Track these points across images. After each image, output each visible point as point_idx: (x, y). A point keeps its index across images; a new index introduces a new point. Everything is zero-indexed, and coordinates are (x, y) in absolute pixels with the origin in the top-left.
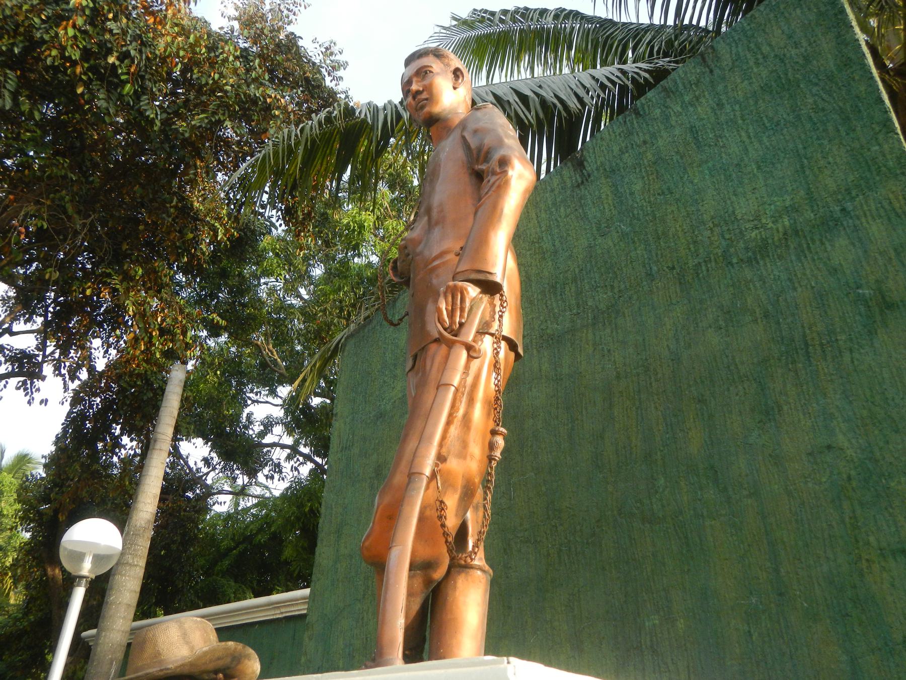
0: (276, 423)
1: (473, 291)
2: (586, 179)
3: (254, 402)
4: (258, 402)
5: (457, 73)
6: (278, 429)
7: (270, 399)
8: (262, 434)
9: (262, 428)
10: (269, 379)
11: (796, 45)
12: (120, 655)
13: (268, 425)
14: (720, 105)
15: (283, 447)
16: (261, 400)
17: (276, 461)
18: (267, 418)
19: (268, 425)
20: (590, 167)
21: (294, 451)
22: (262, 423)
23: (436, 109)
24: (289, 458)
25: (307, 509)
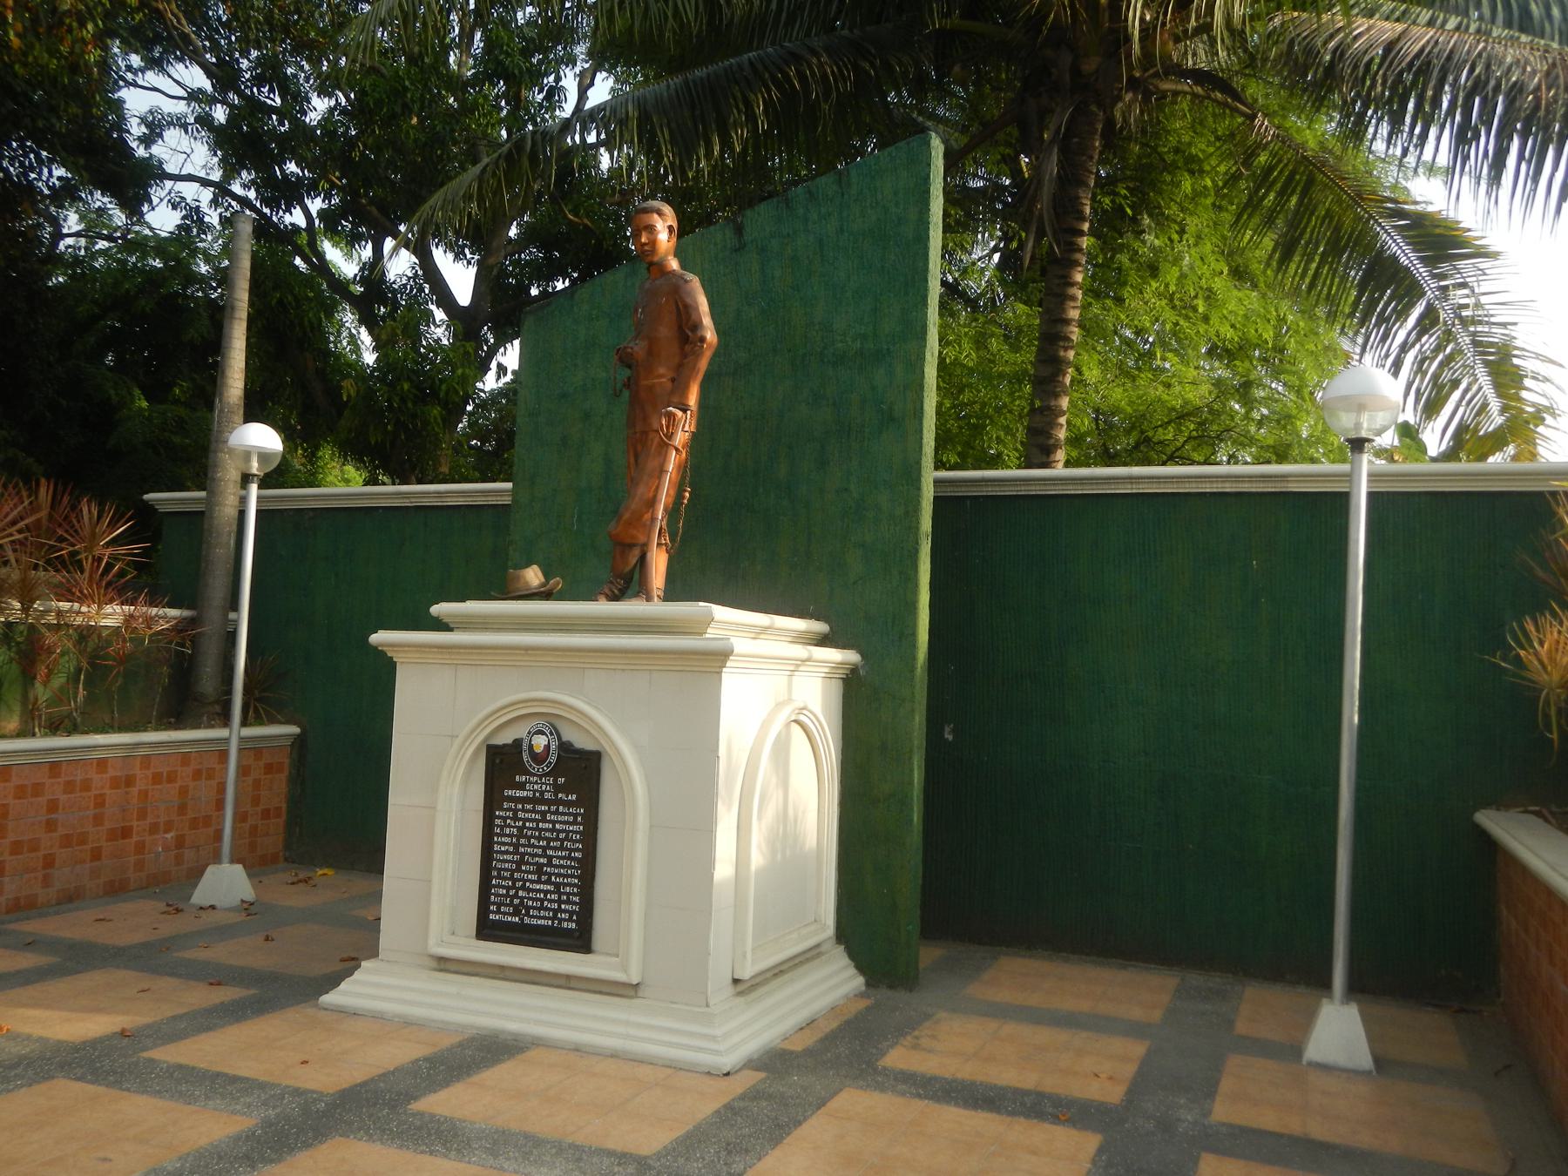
0: (170, 124)
1: (679, 413)
2: (740, 248)
3: (129, 84)
4: (136, 85)
5: (670, 228)
6: (172, 135)
7: (152, 78)
8: (147, 141)
9: (144, 129)
10: (161, 46)
11: (897, 204)
12: (235, 527)
13: (155, 127)
14: (842, 230)
15: (205, 183)
16: (140, 82)
17: (194, 204)
18: (151, 112)
19: (155, 127)
20: (747, 238)
21: (222, 191)
22: (143, 120)
23: (656, 259)
24: (215, 202)
25: (274, 302)
